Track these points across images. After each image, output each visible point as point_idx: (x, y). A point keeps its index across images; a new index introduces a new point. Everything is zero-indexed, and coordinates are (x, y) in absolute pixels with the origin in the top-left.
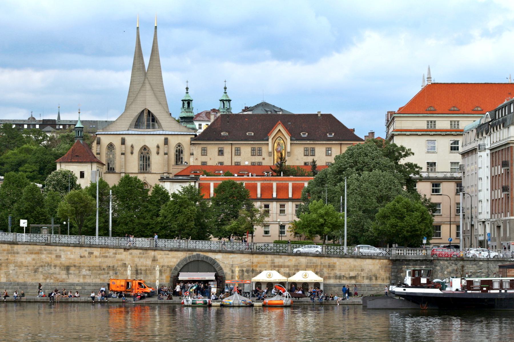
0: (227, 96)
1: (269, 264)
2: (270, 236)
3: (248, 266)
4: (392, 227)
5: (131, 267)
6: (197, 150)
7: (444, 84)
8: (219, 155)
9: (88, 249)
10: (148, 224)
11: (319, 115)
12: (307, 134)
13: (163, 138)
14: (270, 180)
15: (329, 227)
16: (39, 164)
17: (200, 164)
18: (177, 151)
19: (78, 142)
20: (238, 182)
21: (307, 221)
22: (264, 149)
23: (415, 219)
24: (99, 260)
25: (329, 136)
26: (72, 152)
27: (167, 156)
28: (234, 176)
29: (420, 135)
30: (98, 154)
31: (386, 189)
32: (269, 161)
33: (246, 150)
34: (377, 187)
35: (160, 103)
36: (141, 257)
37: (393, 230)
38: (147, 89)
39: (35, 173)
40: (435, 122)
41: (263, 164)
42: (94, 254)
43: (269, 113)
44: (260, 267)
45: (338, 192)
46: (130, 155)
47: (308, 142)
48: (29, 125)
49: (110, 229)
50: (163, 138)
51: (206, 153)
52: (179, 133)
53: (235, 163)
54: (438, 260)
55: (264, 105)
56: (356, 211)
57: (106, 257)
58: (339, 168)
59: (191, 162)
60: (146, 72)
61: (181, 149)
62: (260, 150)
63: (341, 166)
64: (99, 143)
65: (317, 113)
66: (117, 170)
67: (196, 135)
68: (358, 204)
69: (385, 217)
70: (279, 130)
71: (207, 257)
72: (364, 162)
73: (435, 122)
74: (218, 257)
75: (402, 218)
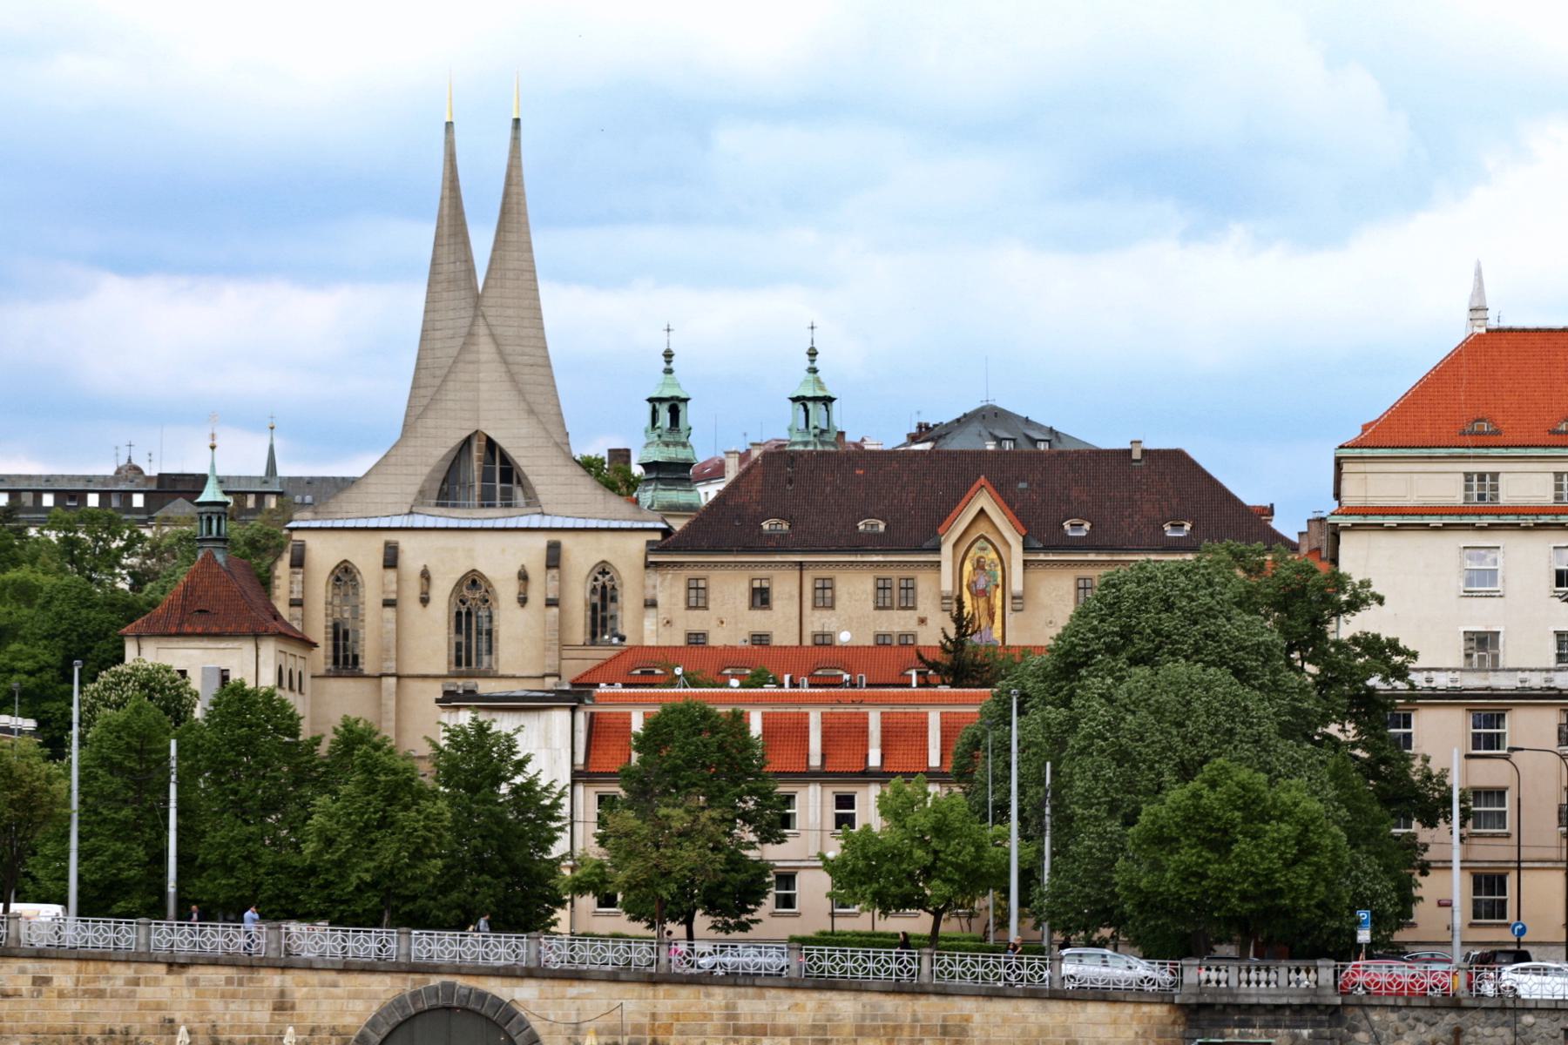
0: (818, 381)
1: (718, 1020)
2: (797, 915)
3: (638, 1029)
4: (1184, 880)
5: (190, 1032)
6: (670, 589)
7: (1538, 330)
8: (753, 606)
9: (32, 966)
10: (312, 871)
11: (1136, 455)
12: (1087, 526)
13: (541, 541)
14: (861, 703)
15: (947, 881)
16: (61, 643)
17: (680, 641)
18: (594, 590)
19: (210, 560)
20: (721, 710)
21: (866, 857)
22: (924, 582)
23: (1271, 850)
24: (73, 1006)
25: (1169, 532)
26: (185, 598)
27: (555, 610)
28: (727, 685)
29: (1436, 529)
30: (294, 603)
31: (1212, 733)
32: (934, 630)
33: (855, 588)
34: (1180, 725)
35: (531, 412)
36: (234, 996)
37: (1192, 892)
38: (483, 357)
39: (47, 676)
40: (1495, 476)
41: (921, 642)
42: (55, 983)
43: (1008, 446)
44: (681, 1033)
45: (1037, 745)
46: (417, 606)
47: (1092, 557)
48: (105, 495)
49: (172, 888)
50: (541, 541)
51: (706, 598)
52: (604, 525)
53: (815, 636)
54: (1362, 1006)
55: (989, 416)
56: (1096, 818)
57: (100, 994)
58: (1067, 654)
59: (647, 633)
60: (479, 290)
61: (609, 584)
62: (909, 588)
63: (1074, 646)
64: (298, 562)
65: (1128, 446)
66: (368, 666)
67: (667, 532)
68: (1106, 793)
69: (1161, 839)
70: (982, 511)
71: (482, 996)
72: (1157, 632)
73: (1495, 476)
74: (523, 994)
75: (1220, 842)
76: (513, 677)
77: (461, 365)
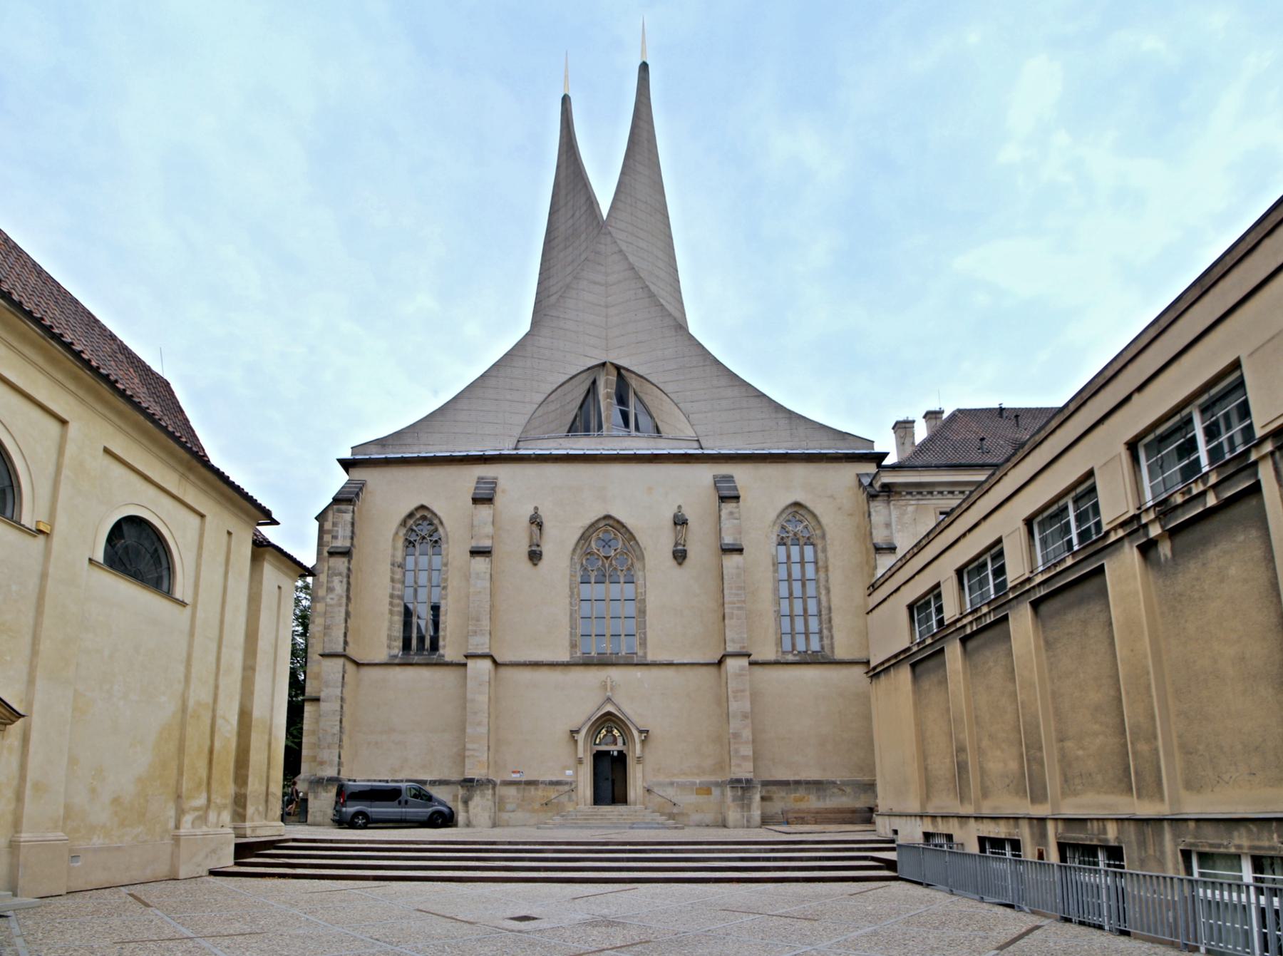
13: (705, 474)
27: (736, 558)
66: (449, 651)
76: (670, 664)
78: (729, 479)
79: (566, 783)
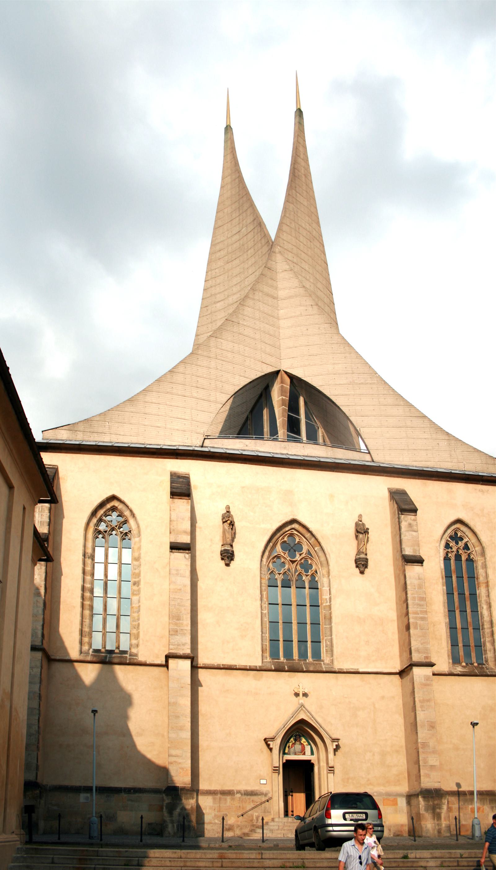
38: (282, 293)
77: (258, 295)
78: (403, 493)
79: (262, 794)
